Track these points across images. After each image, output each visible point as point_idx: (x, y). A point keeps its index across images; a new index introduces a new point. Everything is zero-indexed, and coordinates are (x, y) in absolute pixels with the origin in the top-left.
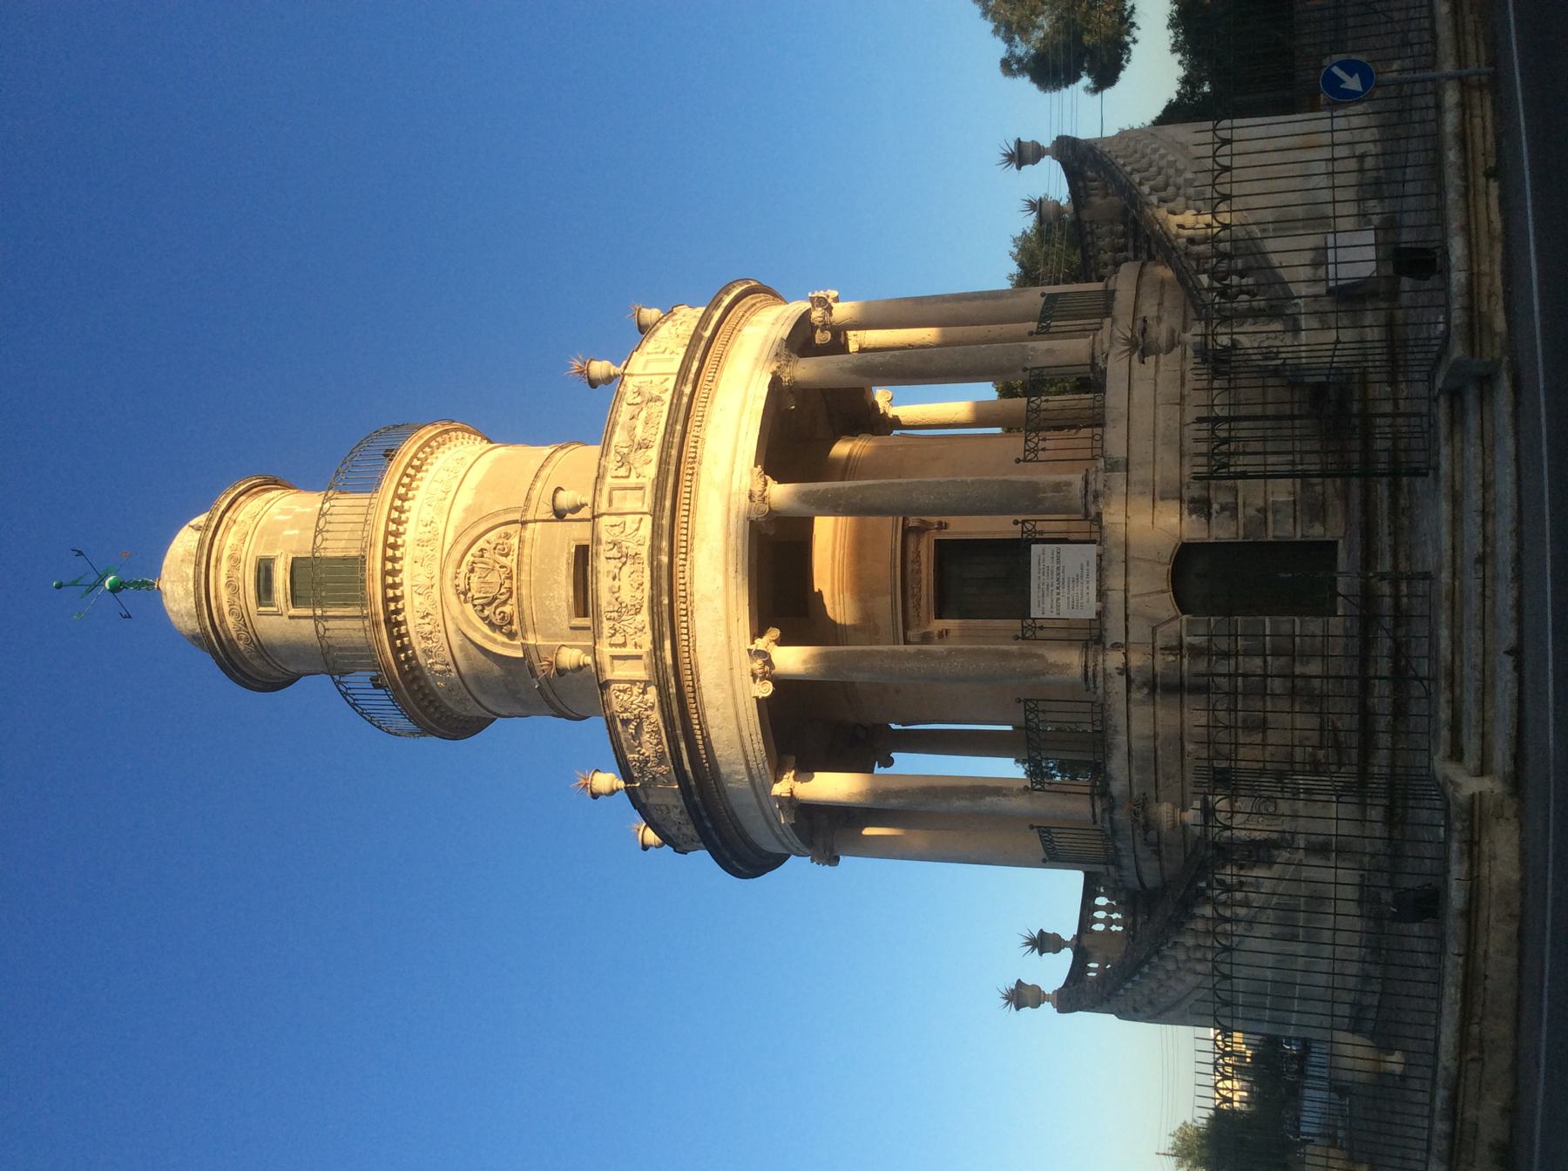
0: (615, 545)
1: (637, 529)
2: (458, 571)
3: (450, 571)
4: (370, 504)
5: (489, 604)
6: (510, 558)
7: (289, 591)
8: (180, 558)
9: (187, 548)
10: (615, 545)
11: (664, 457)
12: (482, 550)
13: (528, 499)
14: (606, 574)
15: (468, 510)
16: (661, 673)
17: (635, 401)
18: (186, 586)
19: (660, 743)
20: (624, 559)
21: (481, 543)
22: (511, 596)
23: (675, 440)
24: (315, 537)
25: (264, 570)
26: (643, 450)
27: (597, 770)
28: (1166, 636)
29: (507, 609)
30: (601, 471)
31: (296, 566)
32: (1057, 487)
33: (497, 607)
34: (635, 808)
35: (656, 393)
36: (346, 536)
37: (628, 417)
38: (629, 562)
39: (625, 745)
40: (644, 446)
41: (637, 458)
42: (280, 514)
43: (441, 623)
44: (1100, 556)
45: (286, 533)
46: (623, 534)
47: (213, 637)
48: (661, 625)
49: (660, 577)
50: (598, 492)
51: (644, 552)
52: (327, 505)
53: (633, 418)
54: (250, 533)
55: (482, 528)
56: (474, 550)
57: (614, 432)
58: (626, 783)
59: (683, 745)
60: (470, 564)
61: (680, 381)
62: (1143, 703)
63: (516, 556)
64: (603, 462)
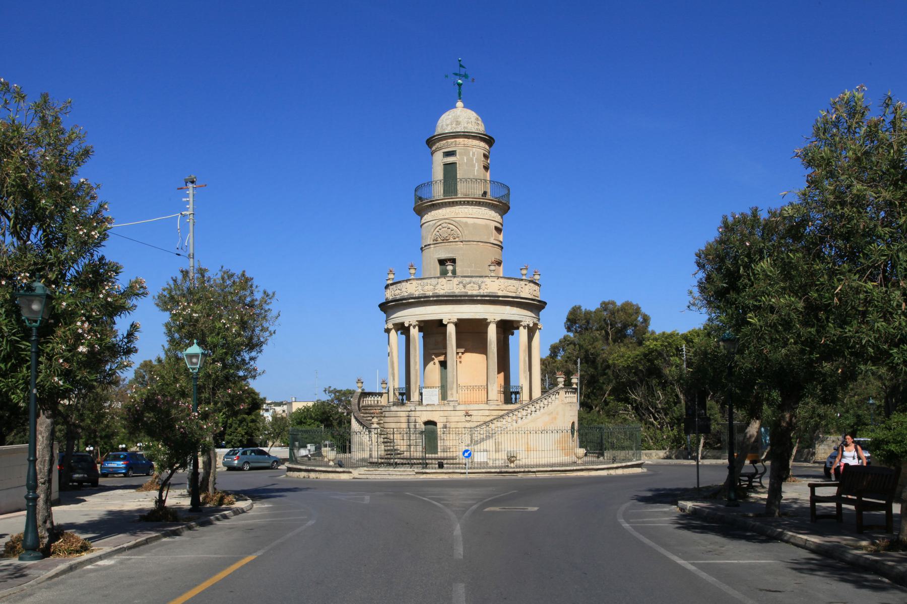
3: (447, 221)
25: (451, 154)
28: (418, 420)
29: (439, 239)
31: (454, 164)
32: (452, 394)
40: (464, 287)
41: (461, 285)
44: (434, 405)
56: (454, 227)
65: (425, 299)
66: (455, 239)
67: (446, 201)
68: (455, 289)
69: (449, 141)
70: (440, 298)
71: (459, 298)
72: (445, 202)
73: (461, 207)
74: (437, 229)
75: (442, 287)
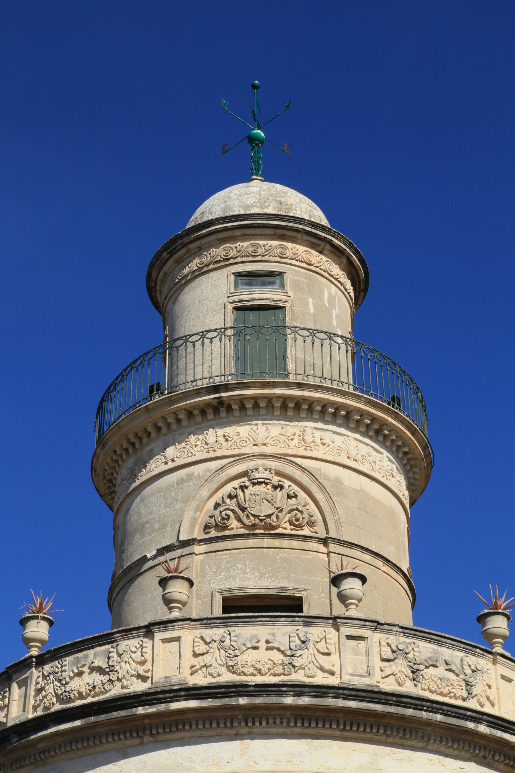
0: (303, 642)
1: (322, 669)
2: (273, 472)
4: (342, 383)
5: (239, 506)
6: (287, 525)
7: (251, 303)
8: (283, 200)
9: (294, 207)
10: (303, 642)
11: (405, 700)
12: (295, 496)
13: (352, 545)
14: (271, 631)
15: (338, 482)
16: (161, 696)
17: (466, 667)
18: (256, 206)
19: (81, 696)
20: (289, 653)
21: (302, 495)
22: (245, 526)
23: (424, 713)
24: (307, 329)
26: (411, 675)
27: (51, 623)
29: (234, 523)
30: (386, 627)
33: (233, 511)
34: (8, 668)
35: (475, 690)
36: (309, 358)
37: (447, 658)
38: (287, 660)
39: (80, 655)
42: (330, 294)
43: (218, 454)
45: (311, 300)
46: (316, 653)
48: (214, 696)
49: (269, 694)
50: (362, 623)
51: (298, 677)
52: (340, 340)
53: (447, 664)
54: (312, 268)
55: (319, 496)
57: (430, 642)
58: (37, 657)
59: (78, 723)
60: (281, 483)
61: (491, 719)
63: (288, 531)
64: (396, 628)
65: (259, 700)
66: (300, 527)
67: (278, 391)
68: (378, 675)
69: (261, 242)
70: (331, 702)
71: (410, 712)
72: (270, 400)
73: (320, 425)
74: (228, 488)
75: (325, 662)
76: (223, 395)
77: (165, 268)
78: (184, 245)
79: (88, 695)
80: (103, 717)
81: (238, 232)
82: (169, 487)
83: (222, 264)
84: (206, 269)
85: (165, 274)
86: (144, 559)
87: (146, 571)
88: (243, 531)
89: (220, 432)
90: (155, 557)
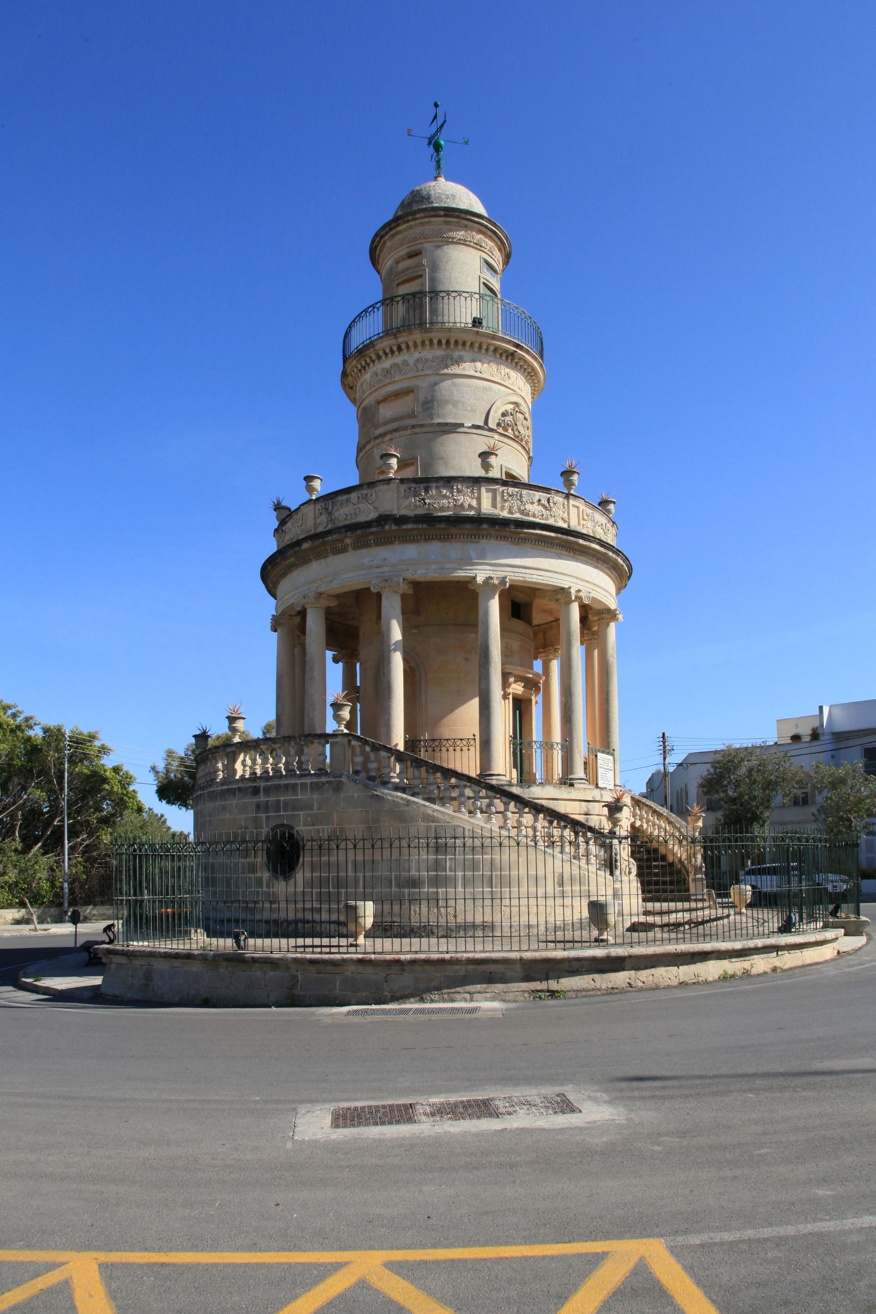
19: (534, 516)
22: (514, 435)
47: (476, 219)
62: (580, 807)
76: (519, 351)
77: (433, 219)
78: (458, 217)
79: (538, 517)
80: (565, 537)
81: (490, 233)
82: (477, 388)
83: (478, 247)
84: (468, 243)
85: (430, 222)
86: (462, 425)
87: (460, 432)
88: (512, 436)
89: (507, 370)
90: (469, 428)
